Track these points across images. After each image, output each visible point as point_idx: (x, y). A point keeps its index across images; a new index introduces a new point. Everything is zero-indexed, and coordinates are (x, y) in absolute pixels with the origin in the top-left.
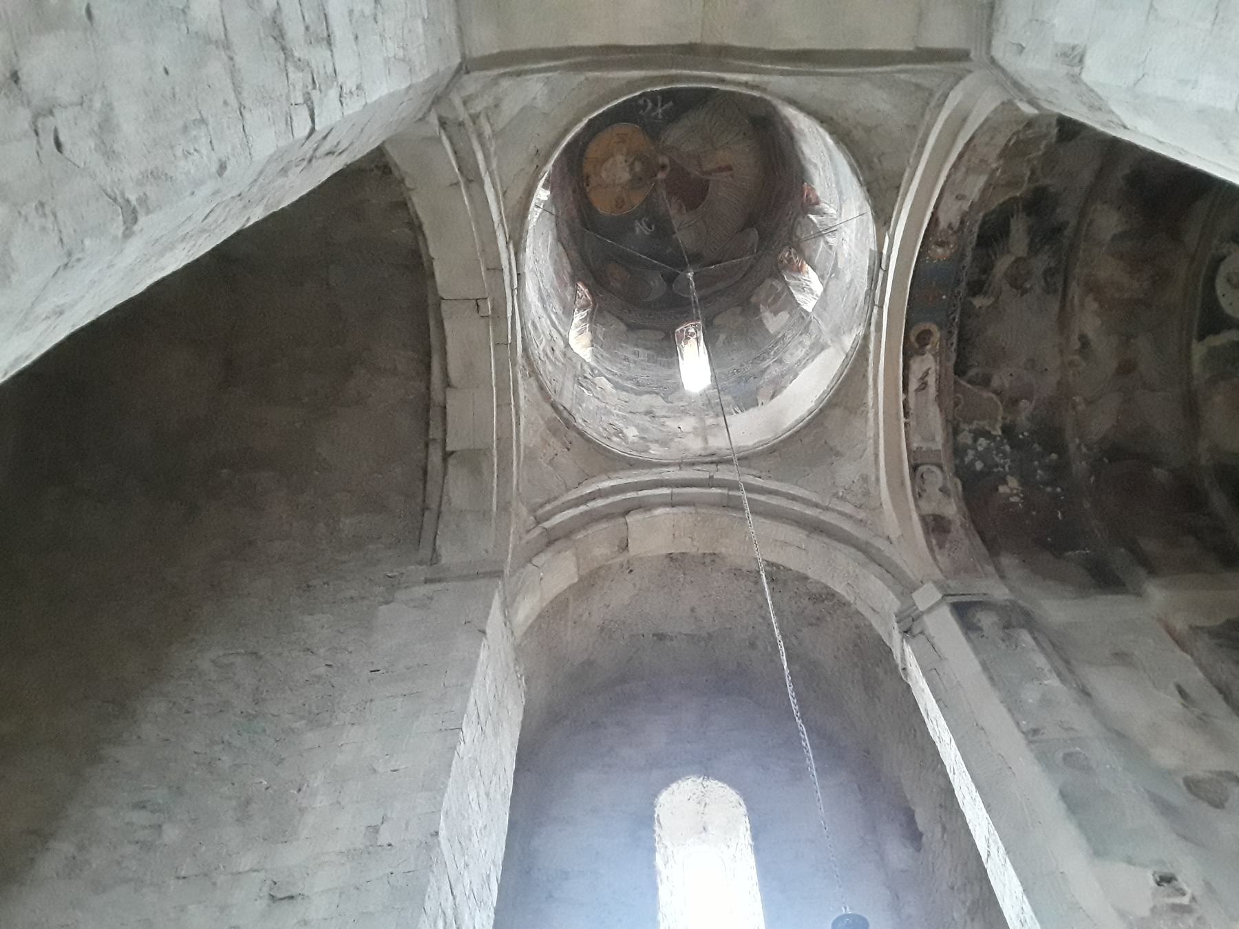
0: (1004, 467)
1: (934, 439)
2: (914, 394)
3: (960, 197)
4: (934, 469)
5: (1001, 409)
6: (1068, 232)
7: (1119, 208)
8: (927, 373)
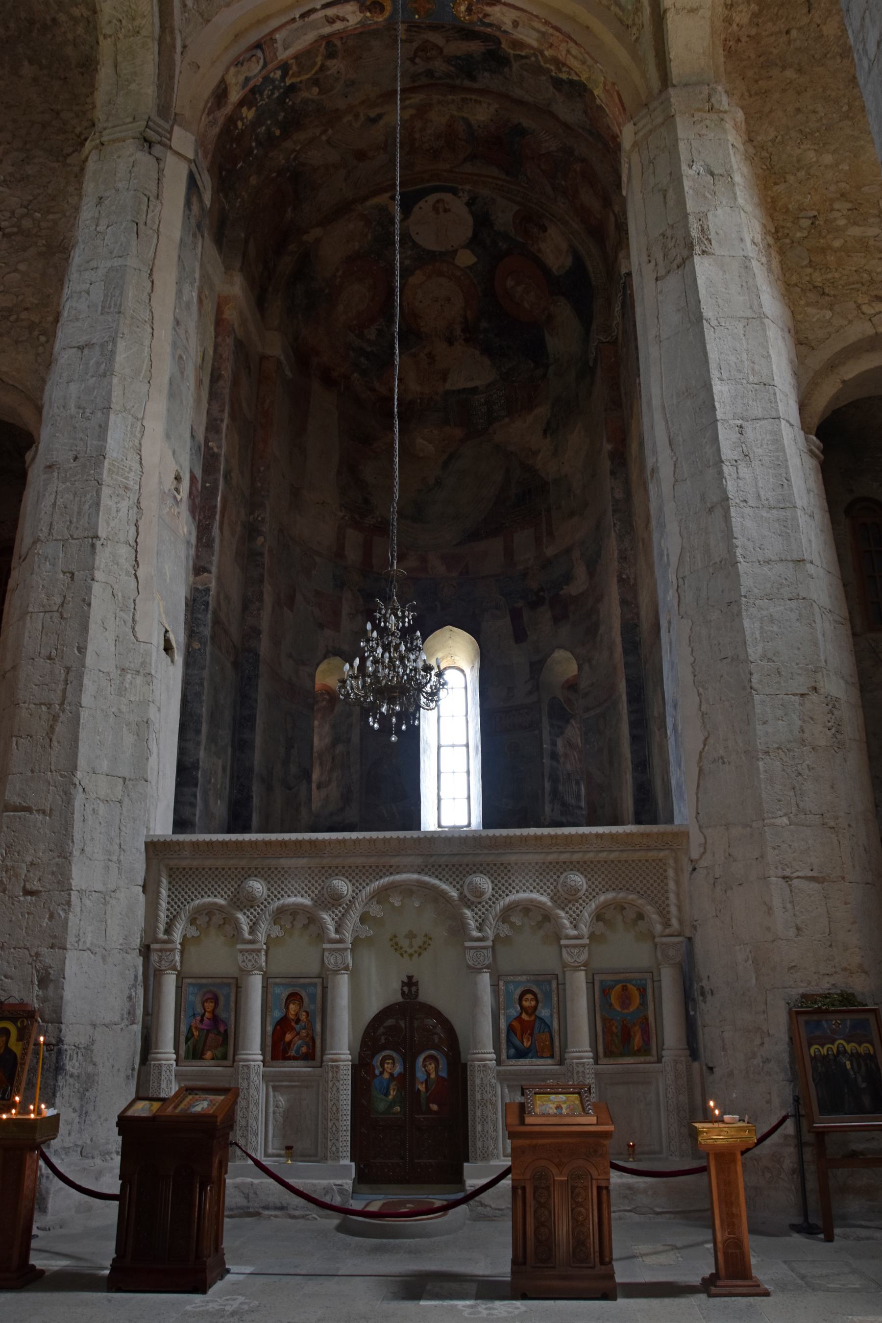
0: (261, 100)
1: (285, 49)
2: (323, 15)
3: (516, 24)
4: (261, 62)
5: (308, 76)
6: (467, 83)
7: (491, 120)
8: (343, 19)
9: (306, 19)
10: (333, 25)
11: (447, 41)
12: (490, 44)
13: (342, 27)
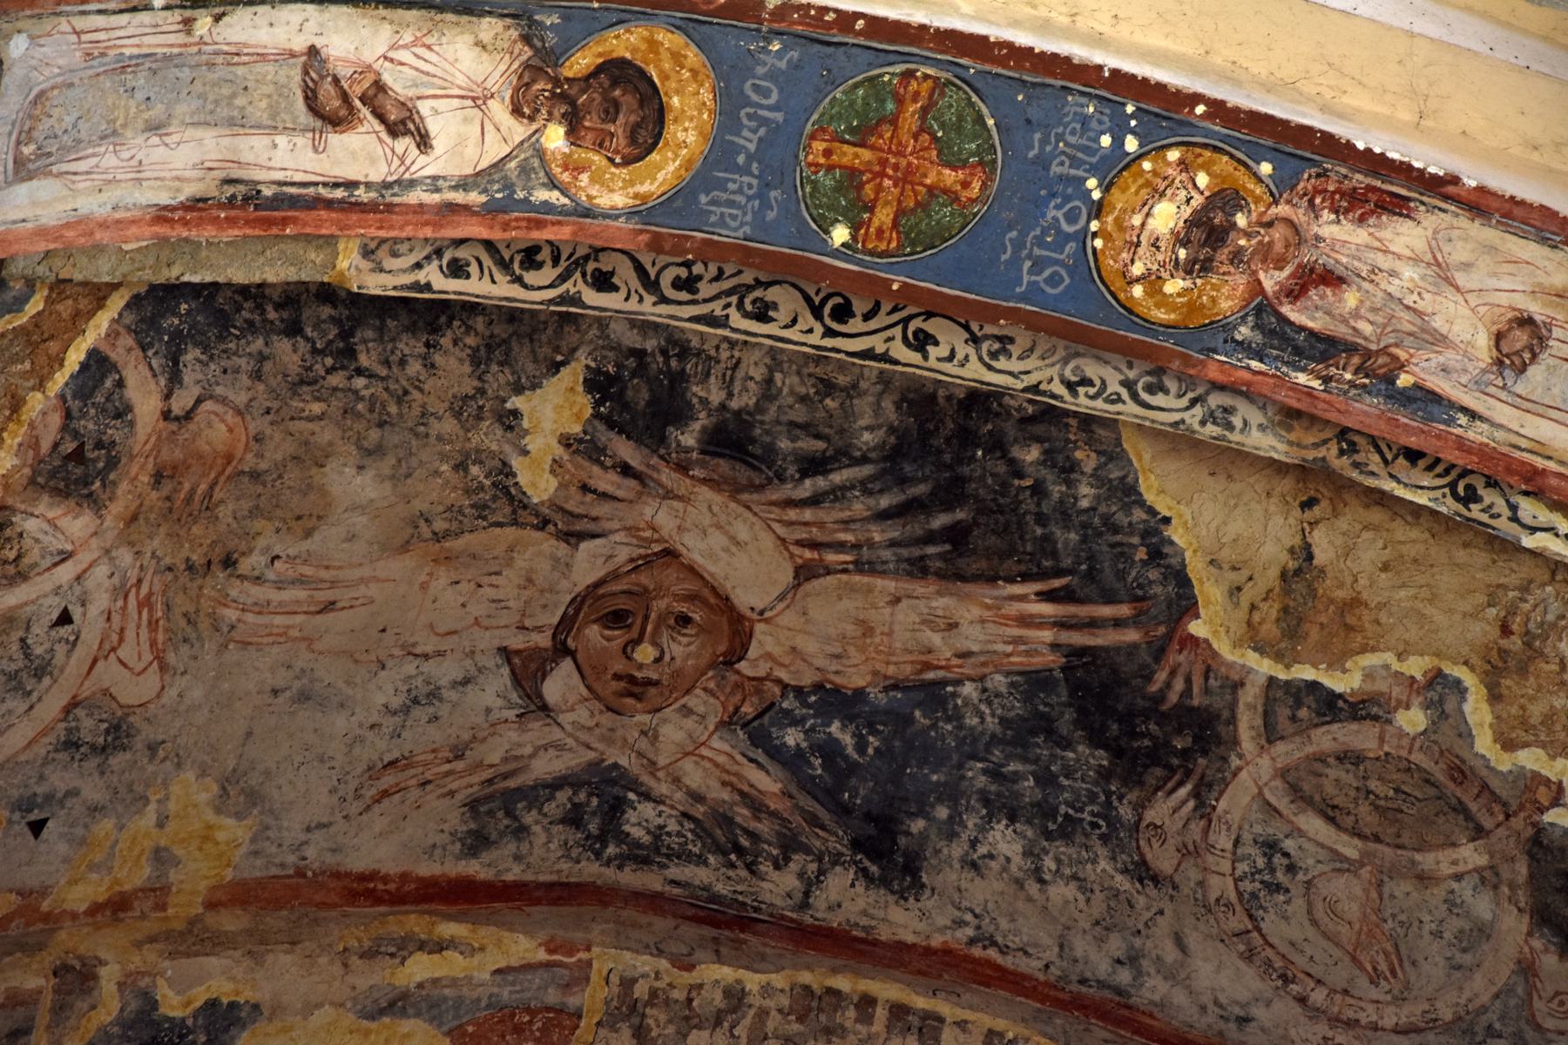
2: (300, 44)
9: (203, 23)
10: (335, 139)
11: (804, 573)
12: (1106, 611)
13: (377, 174)
